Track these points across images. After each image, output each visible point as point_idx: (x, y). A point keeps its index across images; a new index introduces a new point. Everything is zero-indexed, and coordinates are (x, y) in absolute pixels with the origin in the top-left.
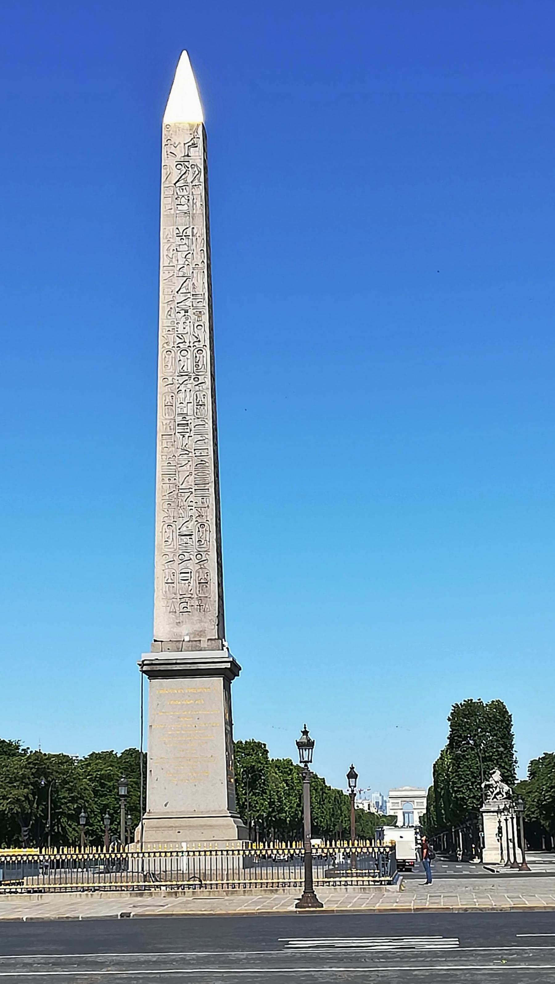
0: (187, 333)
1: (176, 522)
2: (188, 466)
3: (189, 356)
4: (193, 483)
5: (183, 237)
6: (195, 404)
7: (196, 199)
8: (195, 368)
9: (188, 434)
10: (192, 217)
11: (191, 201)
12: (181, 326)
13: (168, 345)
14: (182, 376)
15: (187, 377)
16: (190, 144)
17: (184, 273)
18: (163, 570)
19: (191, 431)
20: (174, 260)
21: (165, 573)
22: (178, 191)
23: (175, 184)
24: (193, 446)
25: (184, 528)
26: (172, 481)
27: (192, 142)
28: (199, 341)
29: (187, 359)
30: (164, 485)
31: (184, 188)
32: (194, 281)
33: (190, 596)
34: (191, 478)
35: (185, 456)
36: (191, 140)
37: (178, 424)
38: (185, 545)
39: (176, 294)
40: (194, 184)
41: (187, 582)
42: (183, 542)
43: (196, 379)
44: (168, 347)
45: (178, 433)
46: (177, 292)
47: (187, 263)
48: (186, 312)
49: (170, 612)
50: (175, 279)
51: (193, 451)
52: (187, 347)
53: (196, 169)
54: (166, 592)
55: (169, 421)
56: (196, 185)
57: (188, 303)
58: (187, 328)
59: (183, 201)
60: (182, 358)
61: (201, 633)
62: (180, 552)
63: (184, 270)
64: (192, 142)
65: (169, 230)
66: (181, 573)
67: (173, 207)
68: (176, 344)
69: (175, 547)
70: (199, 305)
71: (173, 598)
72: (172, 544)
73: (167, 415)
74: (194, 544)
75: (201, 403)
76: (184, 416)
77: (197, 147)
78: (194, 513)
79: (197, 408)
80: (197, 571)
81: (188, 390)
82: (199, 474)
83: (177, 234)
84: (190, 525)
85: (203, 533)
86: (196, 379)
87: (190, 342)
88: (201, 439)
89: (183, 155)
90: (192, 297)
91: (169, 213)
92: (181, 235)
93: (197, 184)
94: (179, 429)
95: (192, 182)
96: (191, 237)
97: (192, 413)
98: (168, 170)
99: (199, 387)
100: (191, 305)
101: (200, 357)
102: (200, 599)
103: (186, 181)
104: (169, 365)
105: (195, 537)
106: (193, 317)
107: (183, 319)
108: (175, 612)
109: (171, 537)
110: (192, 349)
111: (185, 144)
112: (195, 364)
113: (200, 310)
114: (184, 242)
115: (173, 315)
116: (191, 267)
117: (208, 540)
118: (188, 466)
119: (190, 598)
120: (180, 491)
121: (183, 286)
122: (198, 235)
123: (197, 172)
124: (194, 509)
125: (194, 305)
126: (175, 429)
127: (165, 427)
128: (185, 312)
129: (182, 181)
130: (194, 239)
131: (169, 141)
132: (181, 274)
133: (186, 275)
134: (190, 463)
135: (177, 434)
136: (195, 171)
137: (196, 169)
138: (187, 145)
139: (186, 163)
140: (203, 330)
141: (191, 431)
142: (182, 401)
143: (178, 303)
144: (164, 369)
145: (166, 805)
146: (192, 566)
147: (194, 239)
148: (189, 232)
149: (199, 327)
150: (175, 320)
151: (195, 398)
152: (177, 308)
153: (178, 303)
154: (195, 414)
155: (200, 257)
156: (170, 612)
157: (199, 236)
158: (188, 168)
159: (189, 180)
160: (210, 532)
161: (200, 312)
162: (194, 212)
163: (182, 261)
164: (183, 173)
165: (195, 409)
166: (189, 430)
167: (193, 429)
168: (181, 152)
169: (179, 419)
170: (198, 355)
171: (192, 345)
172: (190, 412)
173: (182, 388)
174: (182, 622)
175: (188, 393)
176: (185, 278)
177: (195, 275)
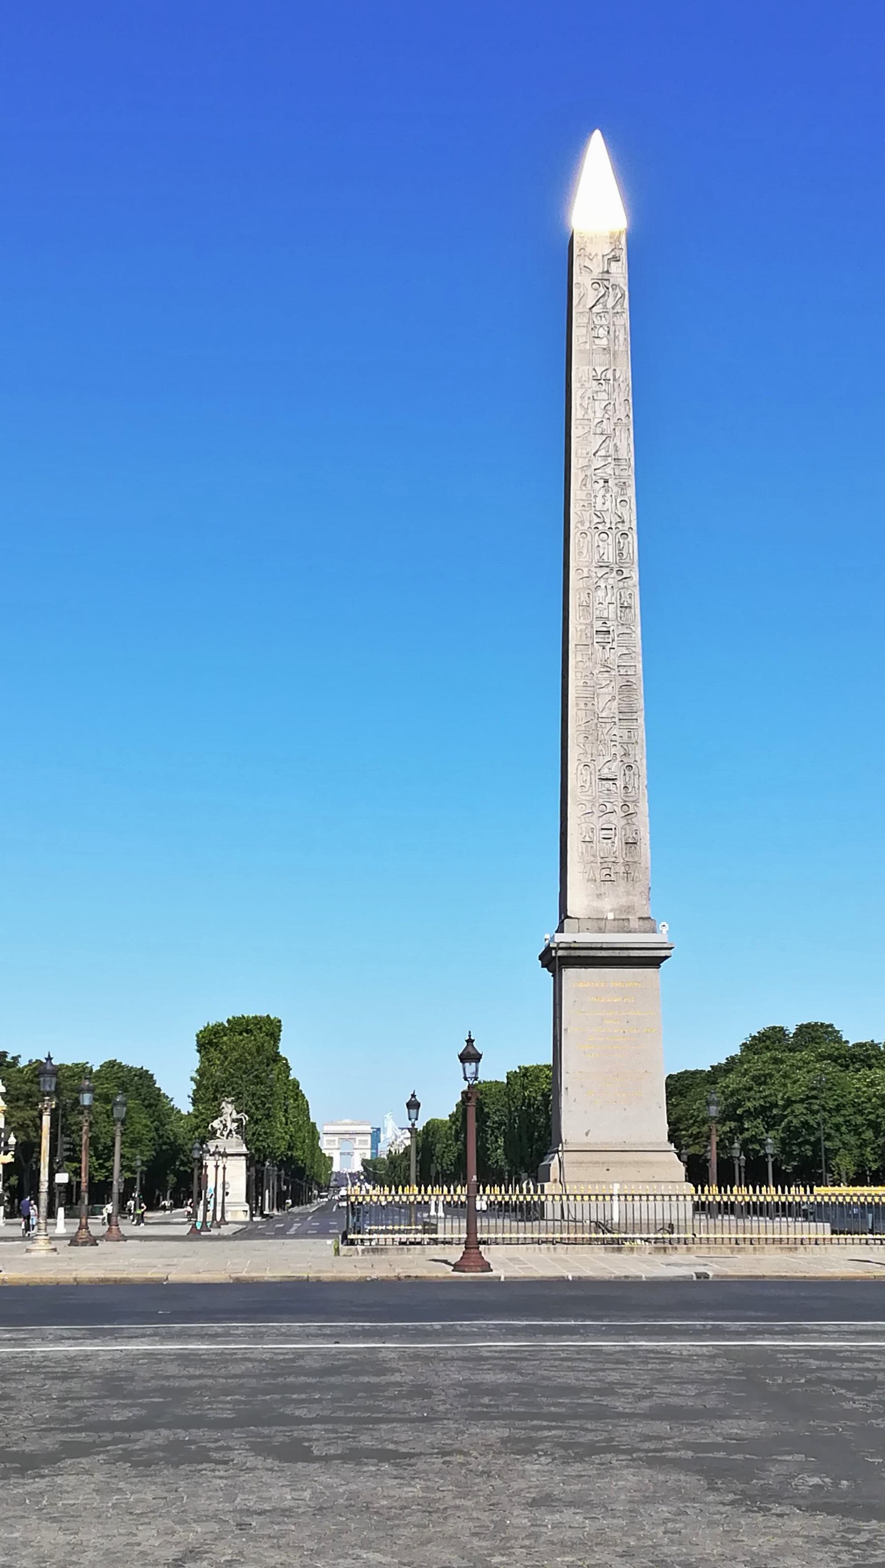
0: (608, 510)
1: (594, 761)
2: (610, 688)
3: (610, 541)
4: (616, 711)
5: (602, 381)
6: (619, 606)
7: (619, 331)
9: (610, 646)
10: (614, 356)
11: (611, 333)
12: (600, 500)
13: (583, 525)
14: (601, 567)
15: (607, 570)
16: (610, 256)
17: (603, 430)
18: (579, 825)
19: (613, 641)
20: (590, 411)
21: (581, 828)
22: (595, 320)
23: (591, 309)
24: (617, 662)
25: (606, 770)
26: (590, 706)
27: (613, 253)
28: (623, 522)
29: (608, 544)
30: (579, 712)
31: (602, 315)
33: (613, 859)
34: (615, 704)
35: (606, 675)
36: (612, 251)
37: (597, 631)
38: (606, 792)
39: (593, 456)
40: (615, 311)
41: (610, 841)
42: (603, 789)
43: (620, 572)
44: (582, 528)
45: (597, 642)
47: (607, 416)
48: (606, 481)
49: (588, 880)
50: (591, 437)
51: (616, 667)
52: (607, 528)
54: (582, 853)
55: (584, 627)
56: (618, 313)
57: (609, 470)
58: (608, 503)
59: (602, 332)
60: (601, 543)
61: (630, 909)
62: (601, 801)
63: (604, 425)
64: (613, 253)
65: (584, 371)
67: (588, 340)
69: (594, 794)
70: (622, 473)
71: (592, 862)
72: (590, 791)
73: (582, 618)
74: (619, 792)
75: (626, 604)
77: (619, 261)
79: (621, 611)
80: (623, 828)
81: (609, 587)
82: (625, 699)
83: (593, 376)
84: (614, 766)
85: (630, 777)
86: (620, 572)
87: (611, 523)
88: (627, 652)
89: (601, 271)
90: (613, 463)
91: (583, 348)
92: (599, 378)
95: (613, 308)
96: (611, 382)
97: (615, 617)
98: (581, 289)
99: (624, 582)
100: (612, 473)
101: (624, 544)
102: (627, 864)
104: (585, 551)
105: (620, 783)
106: (616, 489)
107: (602, 492)
108: (595, 881)
110: (614, 531)
112: (617, 552)
114: (603, 388)
115: (589, 486)
116: (612, 421)
117: (636, 786)
118: (610, 688)
119: (614, 862)
120: (600, 720)
121: (602, 447)
122: (621, 379)
123: (619, 295)
124: (619, 746)
125: (616, 474)
127: (579, 634)
128: (605, 482)
130: (616, 385)
131: (582, 251)
132: (599, 431)
133: (605, 433)
134: (613, 683)
135: (595, 644)
136: (617, 294)
138: (606, 258)
139: (606, 283)
141: (613, 641)
142: (601, 601)
143: (595, 470)
144: (577, 557)
145: (587, 1134)
146: (617, 820)
147: (616, 385)
148: (609, 375)
150: (592, 492)
151: (619, 597)
152: (593, 477)
153: (595, 470)
154: (619, 619)
155: (623, 409)
156: (588, 880)
157: (623, 381)
158: (608, 288)
159: (610, 303)
160: (639, 776)
161: (624, 483)
162: (616, 348)
163: (599, 414)
165: (619, 612)
166: (610, 640)
167: (616, 638)
168: (599, 266)
169: (598, 626)
170: (621, 541)
171: (614, 527)
172: (612, 616)
173: (602, 584)
174: (605, 894)
176: (604, 437)
177: (617, 434)
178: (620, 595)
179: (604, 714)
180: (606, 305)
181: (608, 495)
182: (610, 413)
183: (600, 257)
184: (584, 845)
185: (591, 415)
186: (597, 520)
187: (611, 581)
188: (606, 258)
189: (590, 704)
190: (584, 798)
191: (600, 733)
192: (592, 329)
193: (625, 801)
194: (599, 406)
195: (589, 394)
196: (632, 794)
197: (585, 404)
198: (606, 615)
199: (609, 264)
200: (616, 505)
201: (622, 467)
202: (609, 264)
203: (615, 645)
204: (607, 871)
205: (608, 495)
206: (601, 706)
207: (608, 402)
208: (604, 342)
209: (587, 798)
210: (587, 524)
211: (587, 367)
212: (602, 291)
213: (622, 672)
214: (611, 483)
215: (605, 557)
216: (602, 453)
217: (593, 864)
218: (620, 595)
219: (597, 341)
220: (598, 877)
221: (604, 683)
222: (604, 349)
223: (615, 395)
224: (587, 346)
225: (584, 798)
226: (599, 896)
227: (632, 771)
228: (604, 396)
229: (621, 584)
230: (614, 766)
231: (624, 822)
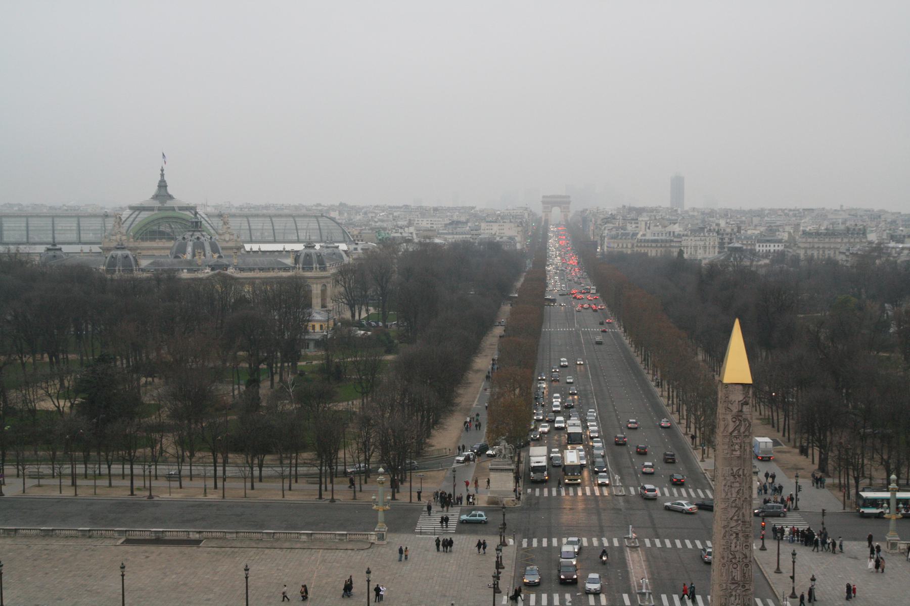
3: (738, 569)
11: (743, 447)
12: (733, 545)
17: (736, 505)
20: (729, 494)
23: (731, 434)
28: (746, 557)
32: (744, 510)
43: (744, 586)
46: (731, 519)
48: (737, 534)
57: (739, 528)
58: (738, 547)
59: (737, 447)
60: (733, 570)
63: (737, 502)
77: (747, 404)
95: (744, 433)
104: (724, 574)
106: (742, 539)
111: (739, 402)
115: (727, 537)
129: (736, 432)
132: (734, 505)
139: (740, 418)
148: (741, 472)
149: (747, 547)
153: (731, 528)
159: (742, 430)
171: (741, 560)
173: (734, 593)
175: (737, 597)
176: (737, 509)
181: (738, 542)
182: (741, 494)
186: (731, 557)
187: (738, 591)
194: (734, 491)
195: (729, 484)
197: (726, 489)
205: (738, 542)
208: (738, 453)
210: (726, 559)
214: (740, 535)
219: (734, 453)
223: (744, 484)
228: (737, 485)
229: (744, 593)
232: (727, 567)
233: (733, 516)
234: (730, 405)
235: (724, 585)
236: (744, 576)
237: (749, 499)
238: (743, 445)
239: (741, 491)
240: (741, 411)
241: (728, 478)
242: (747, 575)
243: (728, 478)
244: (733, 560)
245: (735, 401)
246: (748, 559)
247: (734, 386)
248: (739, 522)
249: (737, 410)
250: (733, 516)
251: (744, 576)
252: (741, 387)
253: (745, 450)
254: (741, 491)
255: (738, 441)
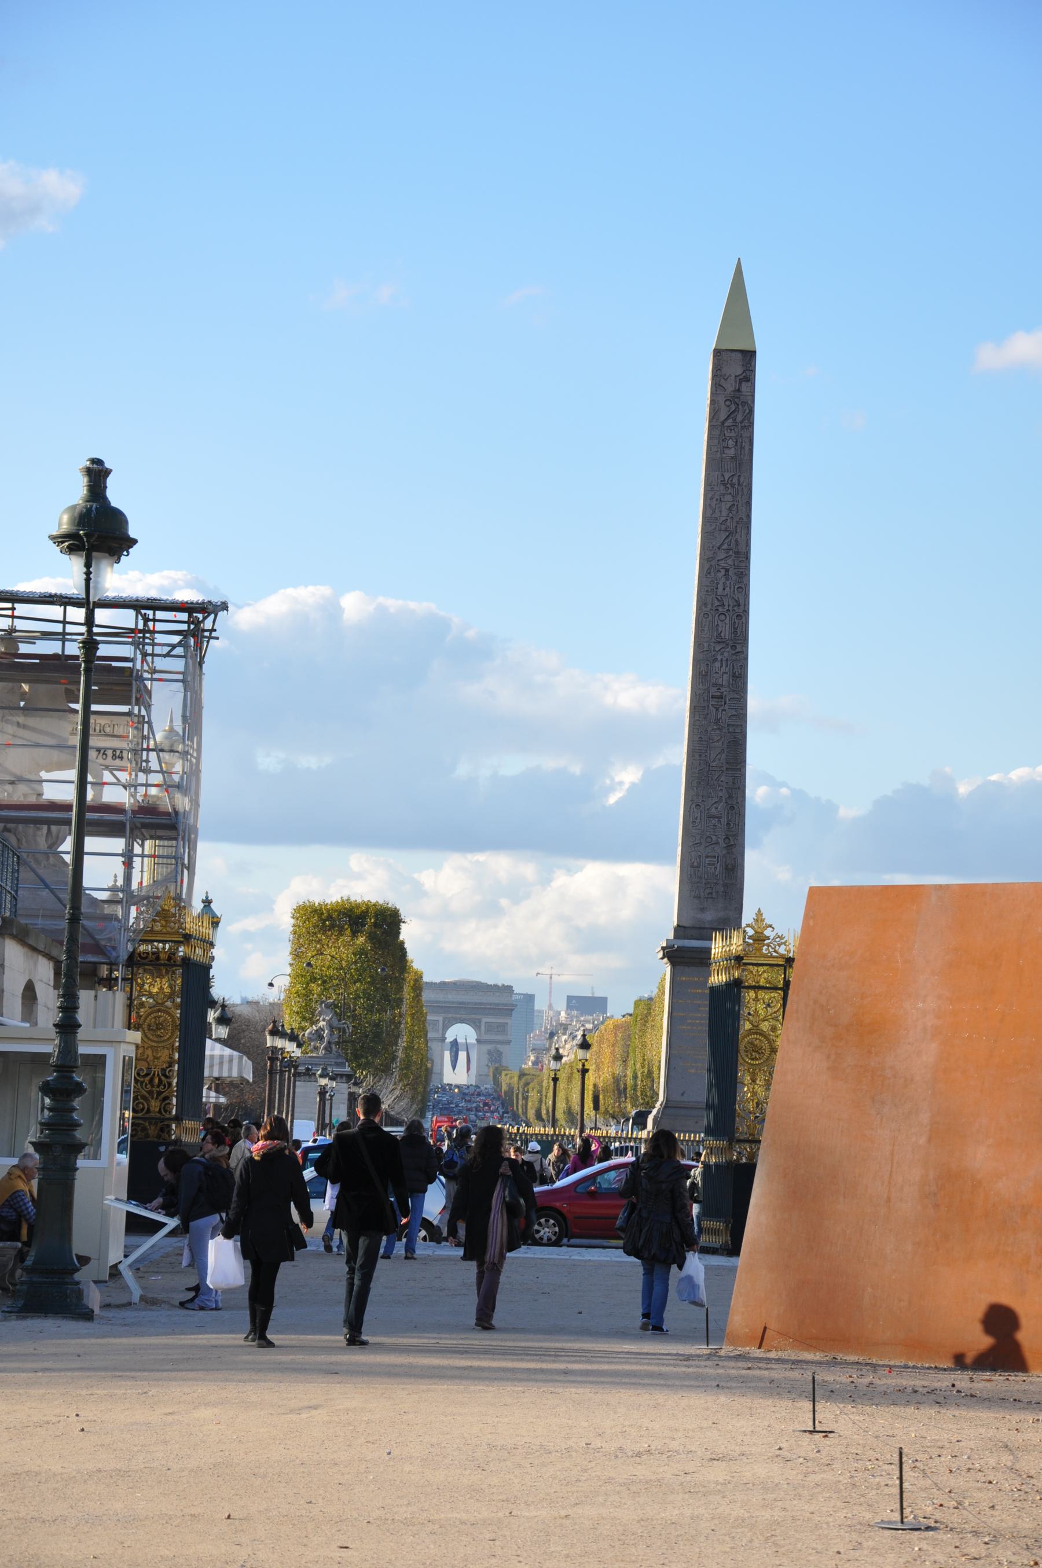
0: (727, 595)
2: (721, 743)
3: (727, 621)
8: (733, 635)
9: (722, 708)
10: (739, 463)
11: (739, 444)
12: (720, 587)
13: (706, 607)
14: (719, 642)
15: (724, 645)
19: (725, 704)
22: (726, 432)
23: (723, 423)
27: (744, 374)
28: (739, 605)
31: (732, 428)
32: (738, 536)
34: (723, 756)
40: (743, 425)
43: (734, 647)
46: (719, 548)
47: (731, 515)
48: (727, 571)
49: (694, 897)
51: (726, 726)
53: (746, 407)
54: (691, 875)
57: (730, 562)
58: (728, 589)
59: (731, 443)
62: (708, 834)
63: (728, 523)
64: (744, 374)
66: (707, 857)
67: (719, 450)
68: (714, 606)
76: (719, 686)
77: (749, 381)
78: (724, 794)
80: (724, 856)
81: (724, 659)
84: (720, 806)
86: (734, 647)
91: (714, 456)
92: (726, 482)
93: (746, 425)
94: (713, 702)
95: (741, 423)
98: (716, 405)
102: (725, 885)
103: (735, 420)
104: (706, 629)
105: (724, 820)
106: (734, 577)
107: (723, 580)
109: (699, 818)
110: (731, 613)
111: (736, 376)
113: (741, 570)
115: (713, 574)
118: (721, 743)
119: (715, 883)
122: (745, 484)
123: (747, 411)
124: (724, 790)
126: (708, 701)
132: (723, 527)
137: (746, 407)
140: (743, 593)
141: (725, 704)
146: (720, 850)
148: (735, 480)
149: (740, 590)
151: (732, 668)
153: (718, 561)
156: (694, 897)
159: (739, 418)
161: (742, 572)
164: (731, 411)
165: (731, 680)
166: (723, 703)
169: (713, 691)
178: (733, 666)
179: (714, 764)
180: (735, 420)
182: (734, 513)
183: (733, 376)
184: (693, 869)
185: (717, 514)
186: (717, 603)
188: (738, 379)
189: (703, 755)
190: (694, 831)
191: (710, 779)
192: (723, 440)
193: (727, 835)
194: (725, 507)
195: (717, 496)
196: (734, 829)
197: (713, 505)
198: (720, 682)
199: (740, 383)
200: (734, 591)
201: (741, 559)
202: (740, 383)
203: (726, 707)
204: (708, 891)
205: (728, 583)
206: (713, 756)
207: (732, 503)
209: (697, 831)
211: (717, 473)
212: (733, 407)
213: (731, 730)
215: (723, 634)
216: (725, 546)
217: (699, 884)
218: (733, 666)
219: (727, 451)
220: (702, 894)
221: (716, 738)
222: (732, 458)
224: (718, 455)
225: (694, 831)
226: (703, 910)
227: (734, 812)
230: (720, 806)
231: (724, 852)
232: (710, 617)
233: (722, 544)
234: (722, 380)
235: (706, 645)
236: (735, 632)
237: (745, 519)
238: (740, 440)
239: (735, 508)
240: (739, 390)
241: (716, 488)
242: (738, 631)
243: (716, 488)
244: (720, 609)
245: (730, 375)
246: (742, 607)
247: (729, 353)
248: (731, 553)
249: (732, 389)
250: (722, 544)
251: (735, 632)
252: (739, 355)
253: (742, 448)
254: (735, 508)
255: (733, 434)
